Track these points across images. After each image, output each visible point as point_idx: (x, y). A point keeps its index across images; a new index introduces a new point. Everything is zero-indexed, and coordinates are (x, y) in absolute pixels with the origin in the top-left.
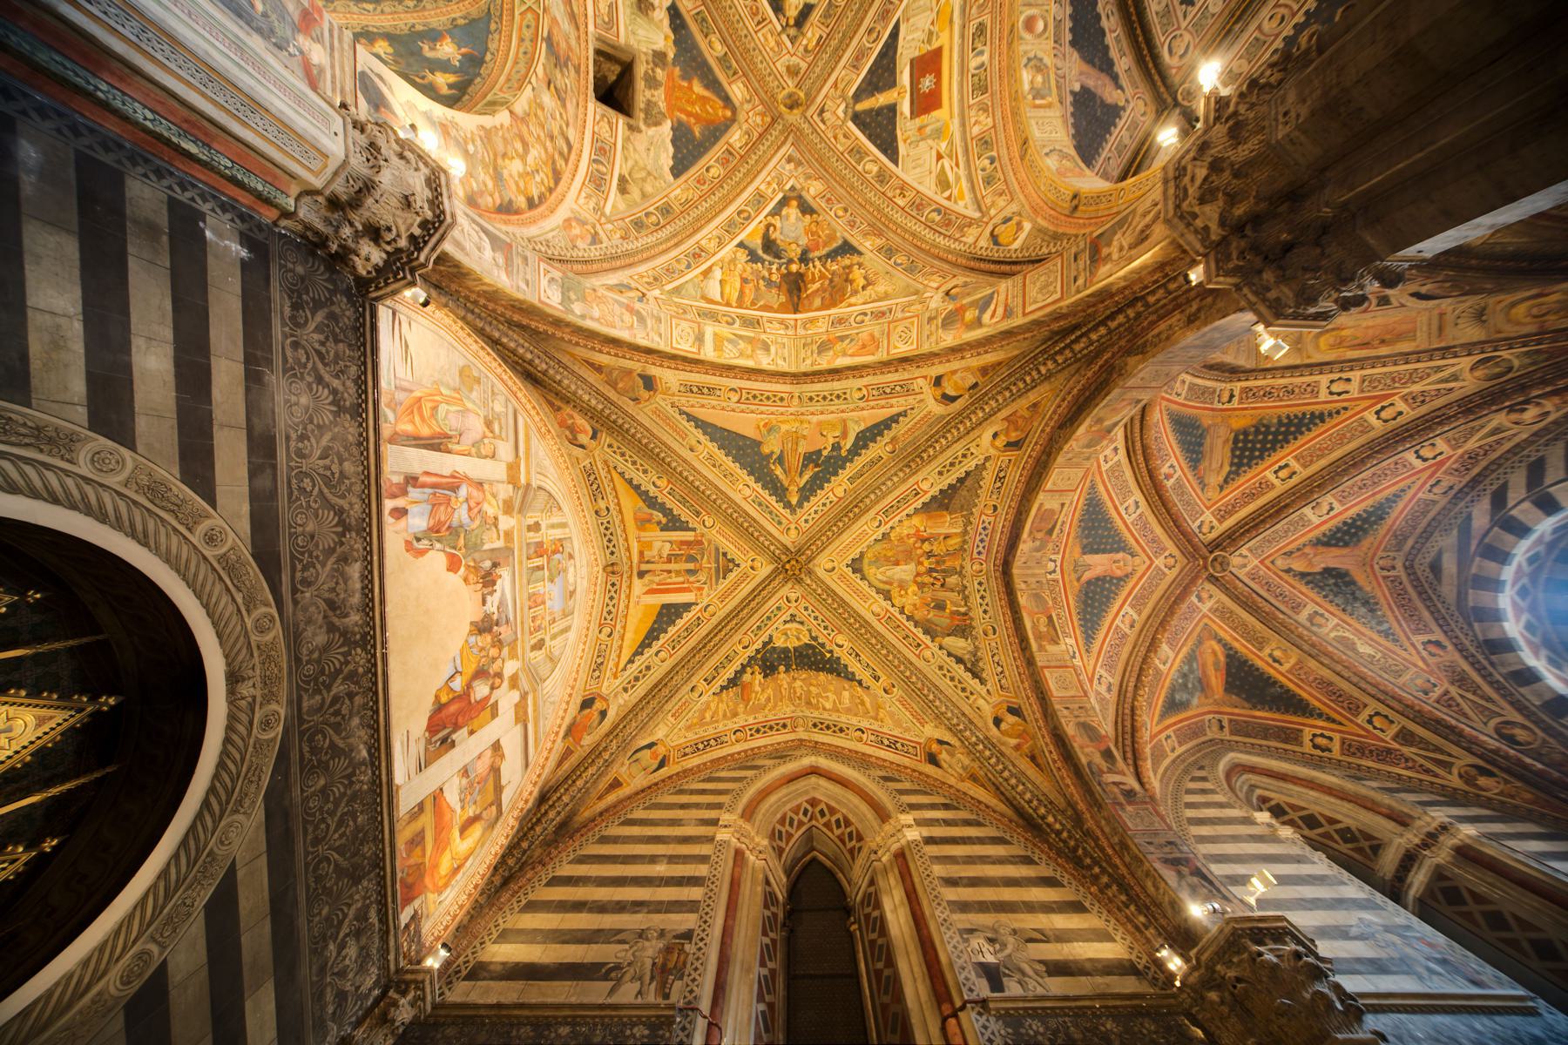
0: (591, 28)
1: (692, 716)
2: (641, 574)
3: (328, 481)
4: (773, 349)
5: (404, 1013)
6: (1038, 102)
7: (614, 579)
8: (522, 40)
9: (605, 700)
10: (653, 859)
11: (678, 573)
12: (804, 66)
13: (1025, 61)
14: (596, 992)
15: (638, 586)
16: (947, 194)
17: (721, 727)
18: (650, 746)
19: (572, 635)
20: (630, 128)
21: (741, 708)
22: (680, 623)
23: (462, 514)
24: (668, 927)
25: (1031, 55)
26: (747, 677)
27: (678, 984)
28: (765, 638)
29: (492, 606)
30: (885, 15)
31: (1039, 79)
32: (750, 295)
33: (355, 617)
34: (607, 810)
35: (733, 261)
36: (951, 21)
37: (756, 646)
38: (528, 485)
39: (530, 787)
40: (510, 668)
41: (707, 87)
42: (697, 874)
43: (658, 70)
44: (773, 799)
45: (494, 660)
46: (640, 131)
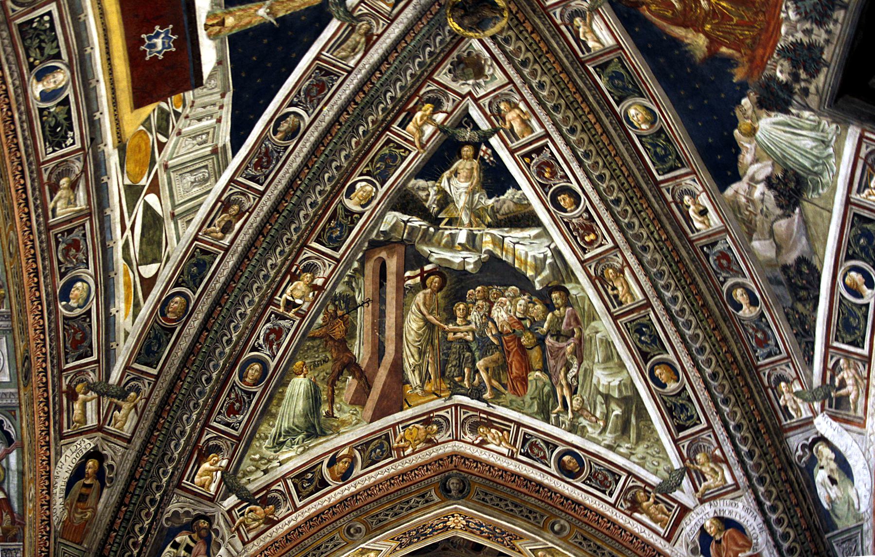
12: (443, 77)
30: (264, 160)
36: (122, 148)
41: (676, 43)
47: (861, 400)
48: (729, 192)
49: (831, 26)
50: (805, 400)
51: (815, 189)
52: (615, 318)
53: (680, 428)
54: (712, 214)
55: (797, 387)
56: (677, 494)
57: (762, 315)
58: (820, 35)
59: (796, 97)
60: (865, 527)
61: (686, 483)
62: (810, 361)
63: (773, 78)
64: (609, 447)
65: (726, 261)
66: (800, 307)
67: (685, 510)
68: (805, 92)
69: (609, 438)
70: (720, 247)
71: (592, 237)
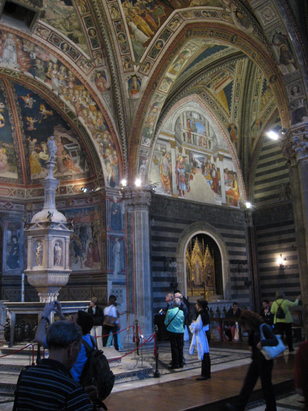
2: (209, 86)
3: (180, 210)
4: (188, 50)
5: (250, 214)
7: (203, 93)
8: (32, 83)
9: (232, 124)
10: (274, 162)
11: (219, 78)
14: (277, 200)
15: (211, 90)
17: (270, 101)
18: (254, 123)
19: (210, 122)
20: (43, 16)
22: (233, 89)
23: (183, 171)
27: (291, 196)
29: (200, 164)
32: (151, 20)
33: (198, 207)
34: (256, 148)
35: (129, 11)
38: (175, 137)
39: (236, 160)
40: (212, 161)
42: (285, 173)
45: (210, 167)
46: (44, 12)
49: (29, 3)
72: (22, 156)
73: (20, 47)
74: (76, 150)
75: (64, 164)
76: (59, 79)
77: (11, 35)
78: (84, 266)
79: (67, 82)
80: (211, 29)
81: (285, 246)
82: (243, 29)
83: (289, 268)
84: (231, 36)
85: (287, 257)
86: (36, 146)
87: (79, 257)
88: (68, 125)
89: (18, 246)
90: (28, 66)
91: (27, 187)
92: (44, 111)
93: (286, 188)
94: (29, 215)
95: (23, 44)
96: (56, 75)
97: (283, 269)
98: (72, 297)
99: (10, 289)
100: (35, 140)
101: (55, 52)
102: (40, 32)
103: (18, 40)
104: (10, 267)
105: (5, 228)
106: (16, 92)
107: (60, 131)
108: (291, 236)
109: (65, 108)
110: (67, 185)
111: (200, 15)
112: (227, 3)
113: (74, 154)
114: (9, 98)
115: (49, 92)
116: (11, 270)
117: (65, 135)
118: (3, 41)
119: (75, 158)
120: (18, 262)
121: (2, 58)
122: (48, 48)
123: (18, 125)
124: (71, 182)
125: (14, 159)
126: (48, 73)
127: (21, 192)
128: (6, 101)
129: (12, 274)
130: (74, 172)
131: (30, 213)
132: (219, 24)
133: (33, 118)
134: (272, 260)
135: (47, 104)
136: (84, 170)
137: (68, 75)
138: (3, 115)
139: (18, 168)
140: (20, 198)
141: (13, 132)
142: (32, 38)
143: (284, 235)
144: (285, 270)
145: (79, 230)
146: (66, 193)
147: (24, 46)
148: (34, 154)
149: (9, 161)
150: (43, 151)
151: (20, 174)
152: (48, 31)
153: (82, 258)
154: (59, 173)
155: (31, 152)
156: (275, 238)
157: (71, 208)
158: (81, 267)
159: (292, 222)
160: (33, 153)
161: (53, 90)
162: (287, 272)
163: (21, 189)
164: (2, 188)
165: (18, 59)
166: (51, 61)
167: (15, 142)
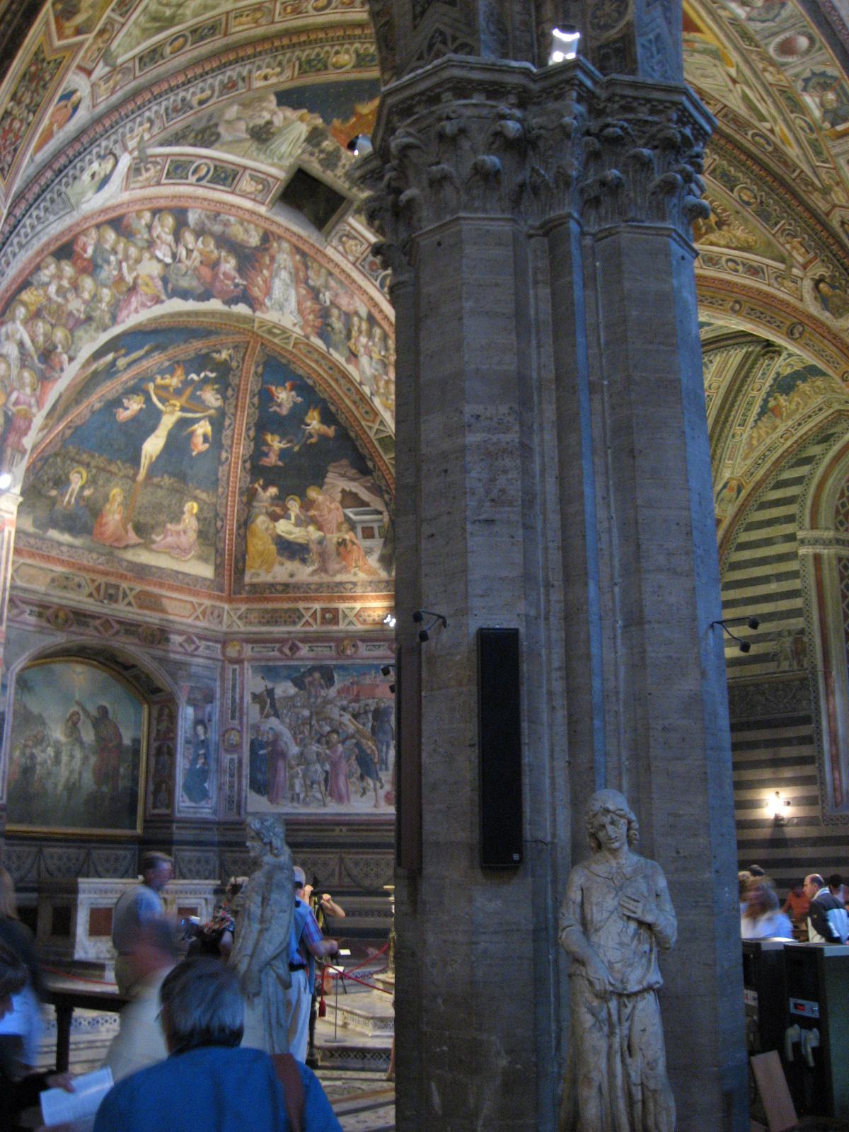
0: (262, 210)
1: (743, 448)
6: (840, 128)
8: (317, 362)
10: (766, 580)
13: (800, 84)
14: (771, 667)
16: (768, 125)
17: (768, 441)
18: (724, 487)
21: (778, 421)
24: (792, 628)
25: (807, 74)
26: (772, 403)
28: (773, 375)
31: (831, 96)
37: (768, 384)
43: (325, 144)
44: (830, 481)
47: (138, 185)
48: (273, 98)
50: (139, 143)
51: (258, 149)
52: (228, 13)
53: (141, 59)
54: (262, 83)
55: (146, 137)
56: (101, 64)
57: (191, 108)
58: (340, 172)
59: (310, 148)
60: (74, 213)
61: (107, 69)
62: (161, 145)
63: (326, 138)
64: (146, 7)
65: (231, 86)
66: (193, 135)
67: (89, 73)
68: (312, 154)
69: (153, 7)
70: (241, 84)
71: (289, 9)
72: (231, 524)
73: (301, 275)
74: (375, 525)
75: (339, 554)
76: (371, 358)
77: (285, 245)
78: (382, 802)
79: (385, 366)
80: (739, 297)
81: (788, 773)
82: (825, 316)
83: (797, 825)
84: (788, 323)
85: (794, 798)
86: (272, 505)
87: (370, 782)
88: (370, 464)
89: (207, 748)
90: (318, 323)
91: (230, 600)
92: (314, 423)
93: (796, 641)
94: (234, 670)
95: (307, 268)
96: (366, 347)
97: (782, 826)
98: (349, 875)
99: (188, 853)
100: (273, 491)
101: (365, 292)
102: (343, 244)
103: (298, 257)
104: (192, 799)
105: (182, 698)
106: (262, 375)
107: (343, 476)
108: (806, 751)
109: (376, 426)
110: (342, 606)
111: (716, 264)
112: (801, 259)
113: (368, 533)
114: (238, 386)
115: (349, 386)
116: (193, 804)
117: (354, 487)
118: (273, 259)
119: (368, 543)
120: (206, 785)
121: (271, 299)
122: (354, 281)
123: (241, 449)
124: (354, 599)
125: (212, 530)
126: (353, 341)
127: (216, 613)
128: (230, 392)
129: (192, 816)
130: (362, 576)
131: (237, 667)
132: (759, 292)
133: (283, 436)
134: (755, 804)
135: (328, 408)
136: (389, 572)
137: (387, 349)
138: (212, 424)
139: (217, 551)
140: (213, 627)
141: (221, 463)
142: (325, 256)
143: (788, 748)
144: (787, 830)
145: (370, 716)
146: (337, 623)
147: (311, 273)
148: (263, 522)
149: (201, 534)
150: (288, 518)
151: (218, 568)
152: (362, 244)
153: (378, 785)
154: (323, 575)
155: (257, 515)
156: (763, 754)
157: (350, 662)
158: (375, 806)
159: (806, 720)
160: (261, 521)
161: (361, 384)
162: (791, 832)
163: (218, 604)
164: (181, 600)
165: (299, 304)
166: (356, 313)
167: (220, 490)
